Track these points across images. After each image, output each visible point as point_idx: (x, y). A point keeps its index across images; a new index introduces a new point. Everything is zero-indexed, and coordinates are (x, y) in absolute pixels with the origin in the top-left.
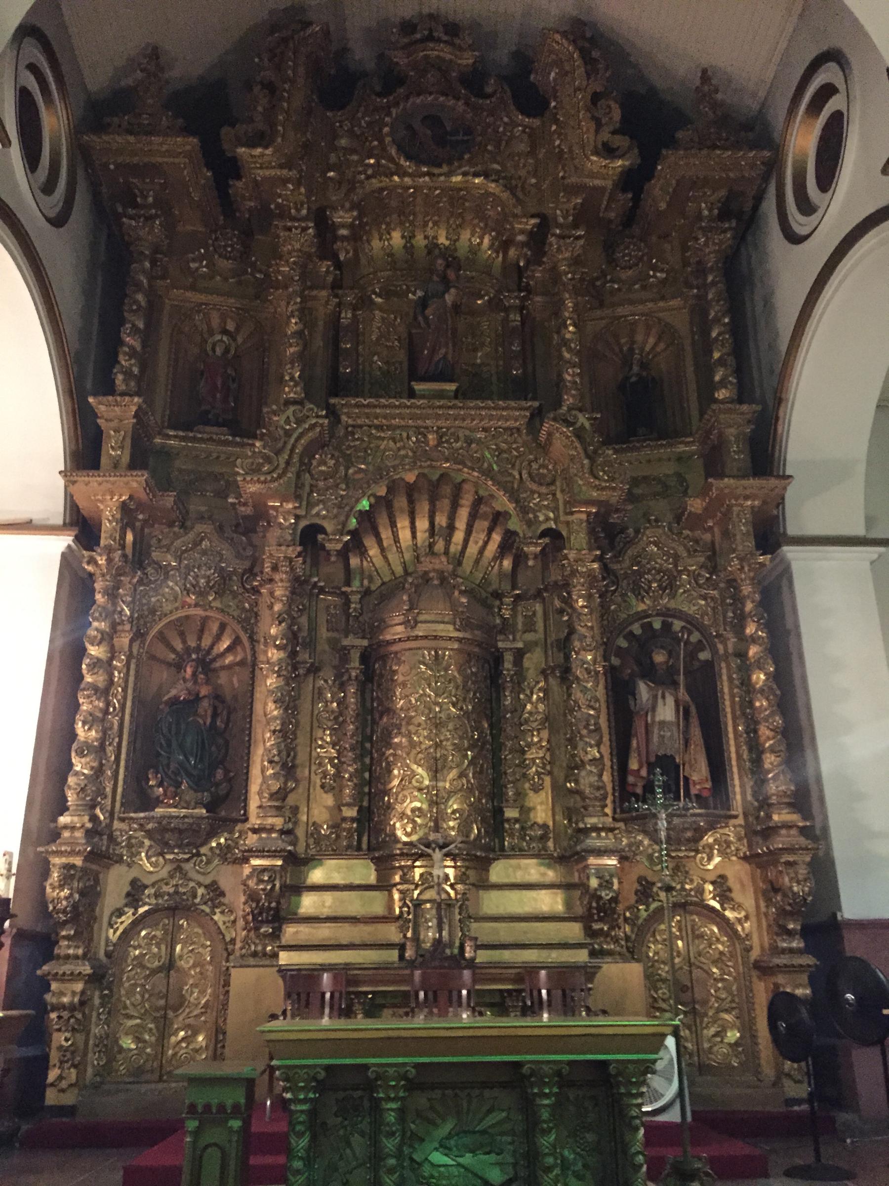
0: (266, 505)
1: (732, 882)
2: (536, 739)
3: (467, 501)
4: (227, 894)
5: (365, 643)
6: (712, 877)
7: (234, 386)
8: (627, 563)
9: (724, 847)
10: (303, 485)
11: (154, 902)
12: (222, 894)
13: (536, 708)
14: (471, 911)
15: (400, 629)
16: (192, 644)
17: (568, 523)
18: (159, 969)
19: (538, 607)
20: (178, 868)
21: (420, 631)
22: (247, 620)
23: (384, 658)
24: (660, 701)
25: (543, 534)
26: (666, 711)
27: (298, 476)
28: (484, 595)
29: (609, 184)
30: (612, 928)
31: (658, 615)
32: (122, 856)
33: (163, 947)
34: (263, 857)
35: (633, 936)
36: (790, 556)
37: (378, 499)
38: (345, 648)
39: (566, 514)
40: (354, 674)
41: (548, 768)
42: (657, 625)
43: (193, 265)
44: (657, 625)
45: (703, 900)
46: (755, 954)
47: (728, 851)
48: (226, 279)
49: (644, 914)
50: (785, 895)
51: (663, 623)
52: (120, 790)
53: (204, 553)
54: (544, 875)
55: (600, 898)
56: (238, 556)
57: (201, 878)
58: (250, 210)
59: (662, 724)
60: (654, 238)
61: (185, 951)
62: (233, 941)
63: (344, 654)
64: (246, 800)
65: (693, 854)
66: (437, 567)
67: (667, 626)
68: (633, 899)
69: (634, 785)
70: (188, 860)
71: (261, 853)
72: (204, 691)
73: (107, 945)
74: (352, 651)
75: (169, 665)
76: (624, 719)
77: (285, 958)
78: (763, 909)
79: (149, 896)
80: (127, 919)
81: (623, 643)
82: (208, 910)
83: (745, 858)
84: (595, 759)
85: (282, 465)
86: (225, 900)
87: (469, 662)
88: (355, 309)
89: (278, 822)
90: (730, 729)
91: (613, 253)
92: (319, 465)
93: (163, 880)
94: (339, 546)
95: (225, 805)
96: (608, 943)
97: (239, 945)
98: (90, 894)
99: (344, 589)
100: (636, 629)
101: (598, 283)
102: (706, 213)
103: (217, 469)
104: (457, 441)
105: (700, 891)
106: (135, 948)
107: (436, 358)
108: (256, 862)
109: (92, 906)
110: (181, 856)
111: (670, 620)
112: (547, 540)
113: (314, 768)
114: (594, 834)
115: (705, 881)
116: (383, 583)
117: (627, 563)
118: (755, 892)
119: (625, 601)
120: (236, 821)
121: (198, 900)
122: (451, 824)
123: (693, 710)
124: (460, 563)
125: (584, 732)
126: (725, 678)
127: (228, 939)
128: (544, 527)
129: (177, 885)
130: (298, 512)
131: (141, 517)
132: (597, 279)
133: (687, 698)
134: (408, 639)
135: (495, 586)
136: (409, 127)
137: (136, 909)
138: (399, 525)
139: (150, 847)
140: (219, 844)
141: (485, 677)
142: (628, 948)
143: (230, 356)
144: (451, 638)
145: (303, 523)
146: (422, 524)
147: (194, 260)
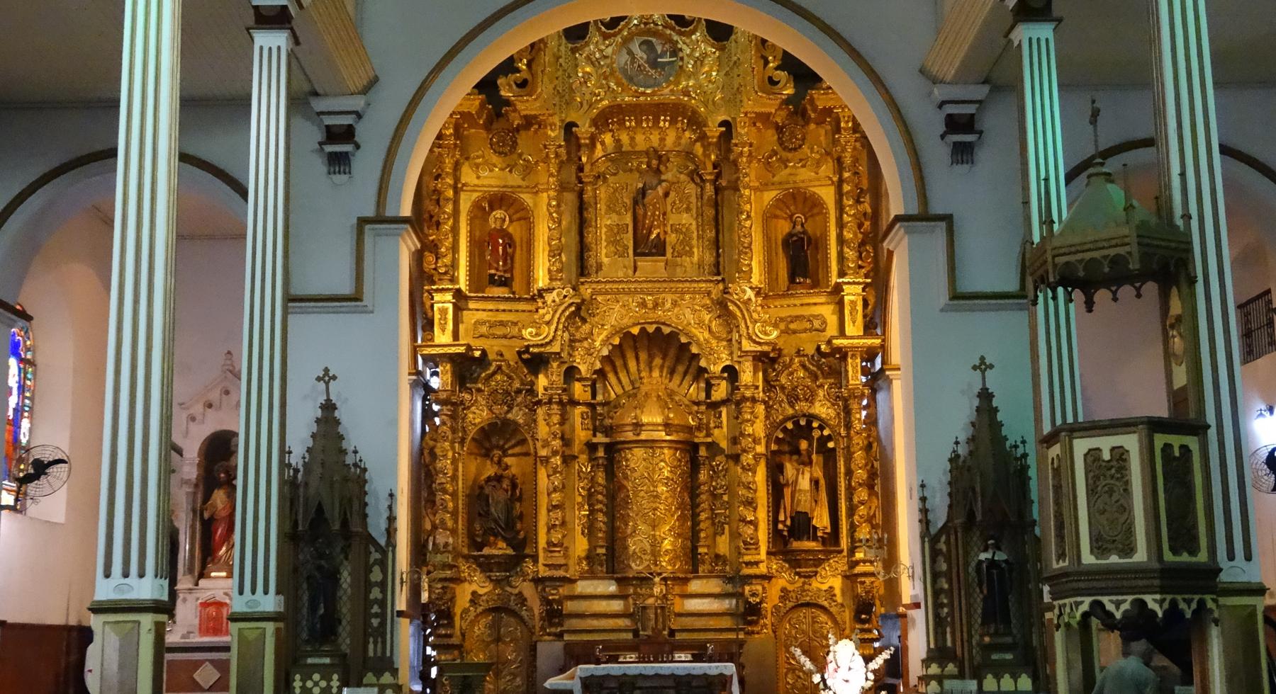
1: (838, 591)
5: (607, 440)
6: (825, 587)
7: (510, 250)
14: (677, 610)
15: (631, 434)
21: (643, 436)
23: (619, 451)
26: (805, 483)
42: (803, 423)
44: (803, 423)
49: (783, 610)
67: (809, 423)
68: (776, 601)
77: (566, 637)
81: (781, 436)
82: (517, 608)
85: (552, 334)
100: (790, 426)
121: (512, 603)
135: (694, 398)
136: (630, 53)
146: (643, 356)
147: (478, 157)
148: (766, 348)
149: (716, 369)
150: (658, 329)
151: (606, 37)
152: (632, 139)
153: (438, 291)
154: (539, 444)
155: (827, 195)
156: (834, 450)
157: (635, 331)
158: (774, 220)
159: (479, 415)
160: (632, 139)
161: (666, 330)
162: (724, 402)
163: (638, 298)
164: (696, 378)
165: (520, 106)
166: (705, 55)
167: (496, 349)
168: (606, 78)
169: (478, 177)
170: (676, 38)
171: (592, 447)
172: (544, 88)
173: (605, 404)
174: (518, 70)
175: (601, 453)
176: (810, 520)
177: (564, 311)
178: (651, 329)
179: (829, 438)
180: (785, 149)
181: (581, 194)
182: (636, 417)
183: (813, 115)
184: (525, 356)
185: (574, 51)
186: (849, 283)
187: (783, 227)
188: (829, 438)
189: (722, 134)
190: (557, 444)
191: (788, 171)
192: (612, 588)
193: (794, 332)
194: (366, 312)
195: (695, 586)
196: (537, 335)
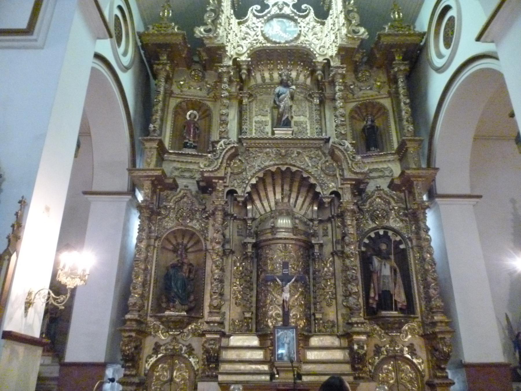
0: (212, 181)
1: (416, 347)
2: (329, 283)
3: (297, 179)
4: (195, 350)
5: (254, 241)
6: (407, 344)
7: (197, 132)
8: (367, 206)
9: (412, 330)
10: (227, 173)
11: (164, 352)
12: (193, 350)
13: (329, 270)
15: (270, 235)
16: (180, 241)
17: (342, 189)
18: (166, 382)
19: (329, 226)
20: (174, 338)
21: (279, 236)
22: (203, 231)
23: (262, 247)
24: (383, 266)
25: (332, 193)
26: (386, 271)
27: (225, 169)
28: (306, 220)
29: (356, 47)
30: (363, 367)
31: (381, 229)
32: (151, 332)
33: (169, 372)
34: (211, 334)
35: (373, 371)
36: (439, 202)
37: (260, 178)
38: (245, 243)
39: (342, 184)
40: (249, 254)
41: (334, 296)
42: (381, 232)
43: (182, 83)
44: (381, 232)
45: (403, 355)
46: (426, 378)
47: (414, 333)
48: (195, 88)
50: (440, 352)
51: (384, 232)
52: (150, 304)
53: (185, 202)
54: (333, 343)
55: (359, 353)
56: (200, 204)
57: (184, 343)
58: (205, 60)
59: (384, 276)
60: (375, 69)
61: (178, 373)
62: (198, 370)
63: (245, 245)
64: (203, 309)
65: (399, 334)
66: (285, 208)
67: (386, 233)
69: (372, 304)
70: (179, 335)
71: (210, 332)
72: (185, 261)
73: (145, 371)
74: (249, 245)
75: (170, 250)
76: (368, 274)
78: (430, 358)
79: (162, 350)
80: (153, 360)
81: (366, 241)
82: (186, 356)
83: (422, 336)
84: (356, 292)
85: (219, 164)
86: (194, 352)
87: (299, 249)
88: (248, 98)
89: (218, 319)
90: (415, 279)
91: (358, 74)
92: (234, 164)
93: (168, 343)
94: (243, 199)
95: (194, 310)
96: (362, 374)
97: (200, 372)
98: (138, 348)
99: (245, 217)
100: (373, 235)
101: (352, 87)
102: (397, 58)
103: (191, 167)
104: (293, 153)
105: (402, 351)
106: (157, 372)
107: (284, 119)
108: (208, 336)
109: (139, 353)
110: (176, 333)
111: (387, 230)
112: (333, 196)
113: (232, 295)
114: (356, 325)
115: (404, 346)
116: (261, 215)
117: (367, 206)
118: (426, 351)
119: (367, 223)
120: (199, 318)
121: (183, 352)
122: (292, 320)
123: (398, 270)
124: (295, 206)
125: (351, 280)
126: (412, 256)
127: (196, 369)
128: (331, 191)
129: (174, 346)
130: (225, 184)
131: (159, 187)
132: (351, 85)
133: (395, 265)
134: (273, 239)
135: (310, 217)
137: (157, 356)
138: (268, 190)
139: (163, 329)
140: (192, 328)
141: (306, 256)
142: (370, 376)
143: (196, 120)
144: (292, 239)
145: (227, 189)
146: (278, 190)
147: (182, 81)
148: (360, 177)
149: (327, 193)
150: (288, 169)
151: (258, 17)
152: (271, 76)
153: (147, 140)
154: (208, 243)
155: (387, 103)
156: (404, 250)
157: (273, 169)
158: (354, 121)
159: (170, 224)
160: (271, 76)
161: (294, 169)
162: (329, 220)
163: (274, 150)
164: (311, 204)
165: (206, 42)
166: (314, 27)
167: (185, 184)
168: (257, 36)
169: (182, 91)
170: (296, 17)
171: (245, 245)
172: (221, 31)
173: (253, 219)
174: (205, 24)
175: (250, 250)
176: (391, 296)
177: (227, 152)
178: (284, 168)
179: (400, 242)
180: (359, 81)
181: (240, 102)
182: (273, 223)
183: (378, 56)
184: (202, 184)
185: (239, 23)
186: (410, 140)
187: (360, 125)
188: (400, 242)
189: (324, 67)
190: (218, 237)
191: (362, 92)
192: (255, 342)
193: (373, 178)
194: (36, 48)
195: (314, 341)
196: (209, 166)
